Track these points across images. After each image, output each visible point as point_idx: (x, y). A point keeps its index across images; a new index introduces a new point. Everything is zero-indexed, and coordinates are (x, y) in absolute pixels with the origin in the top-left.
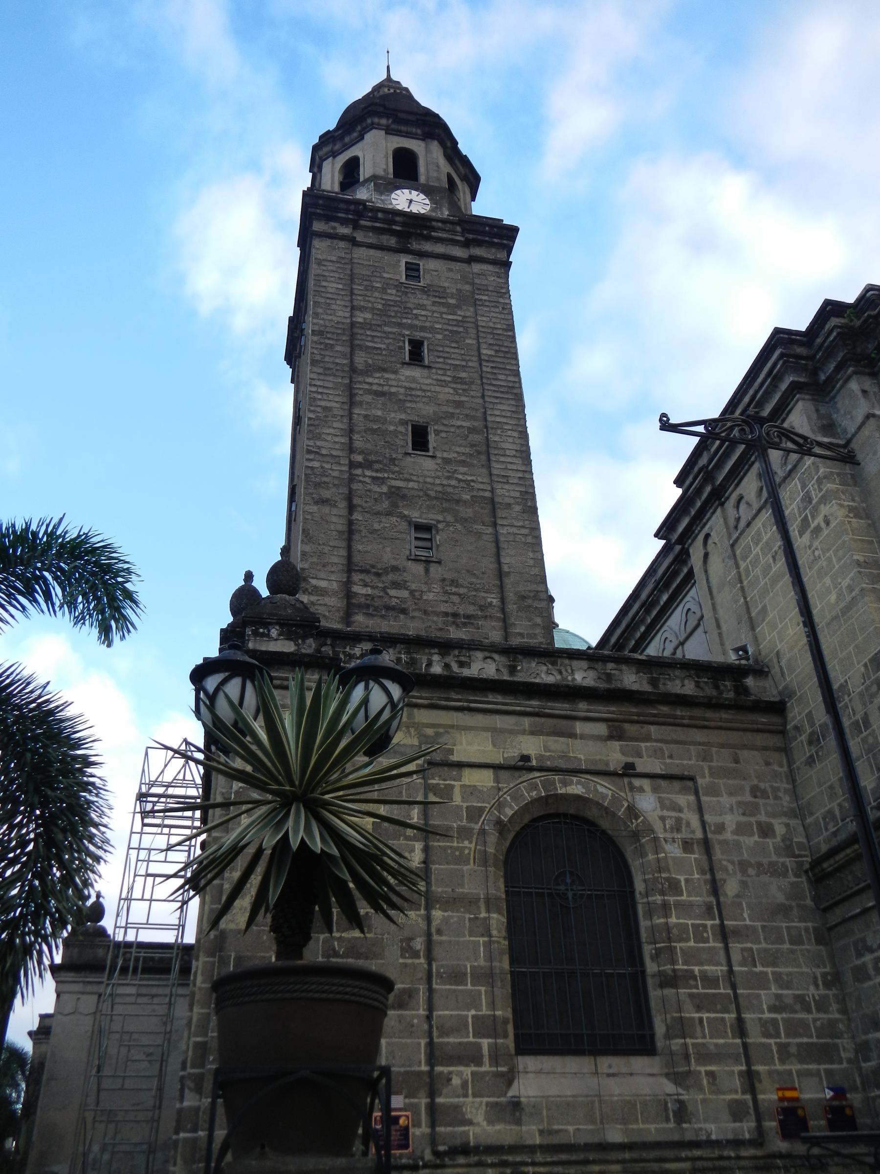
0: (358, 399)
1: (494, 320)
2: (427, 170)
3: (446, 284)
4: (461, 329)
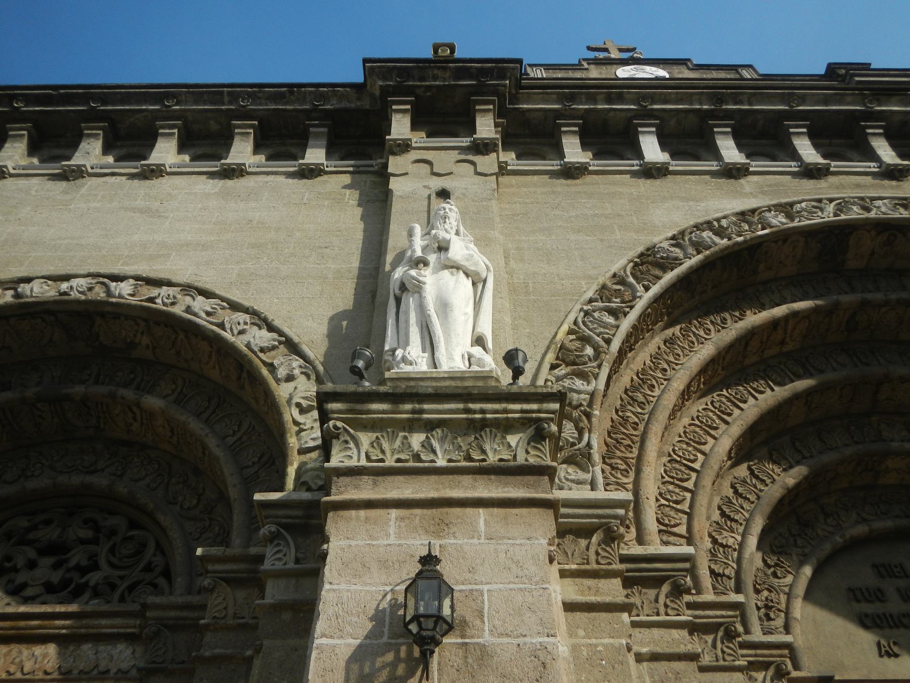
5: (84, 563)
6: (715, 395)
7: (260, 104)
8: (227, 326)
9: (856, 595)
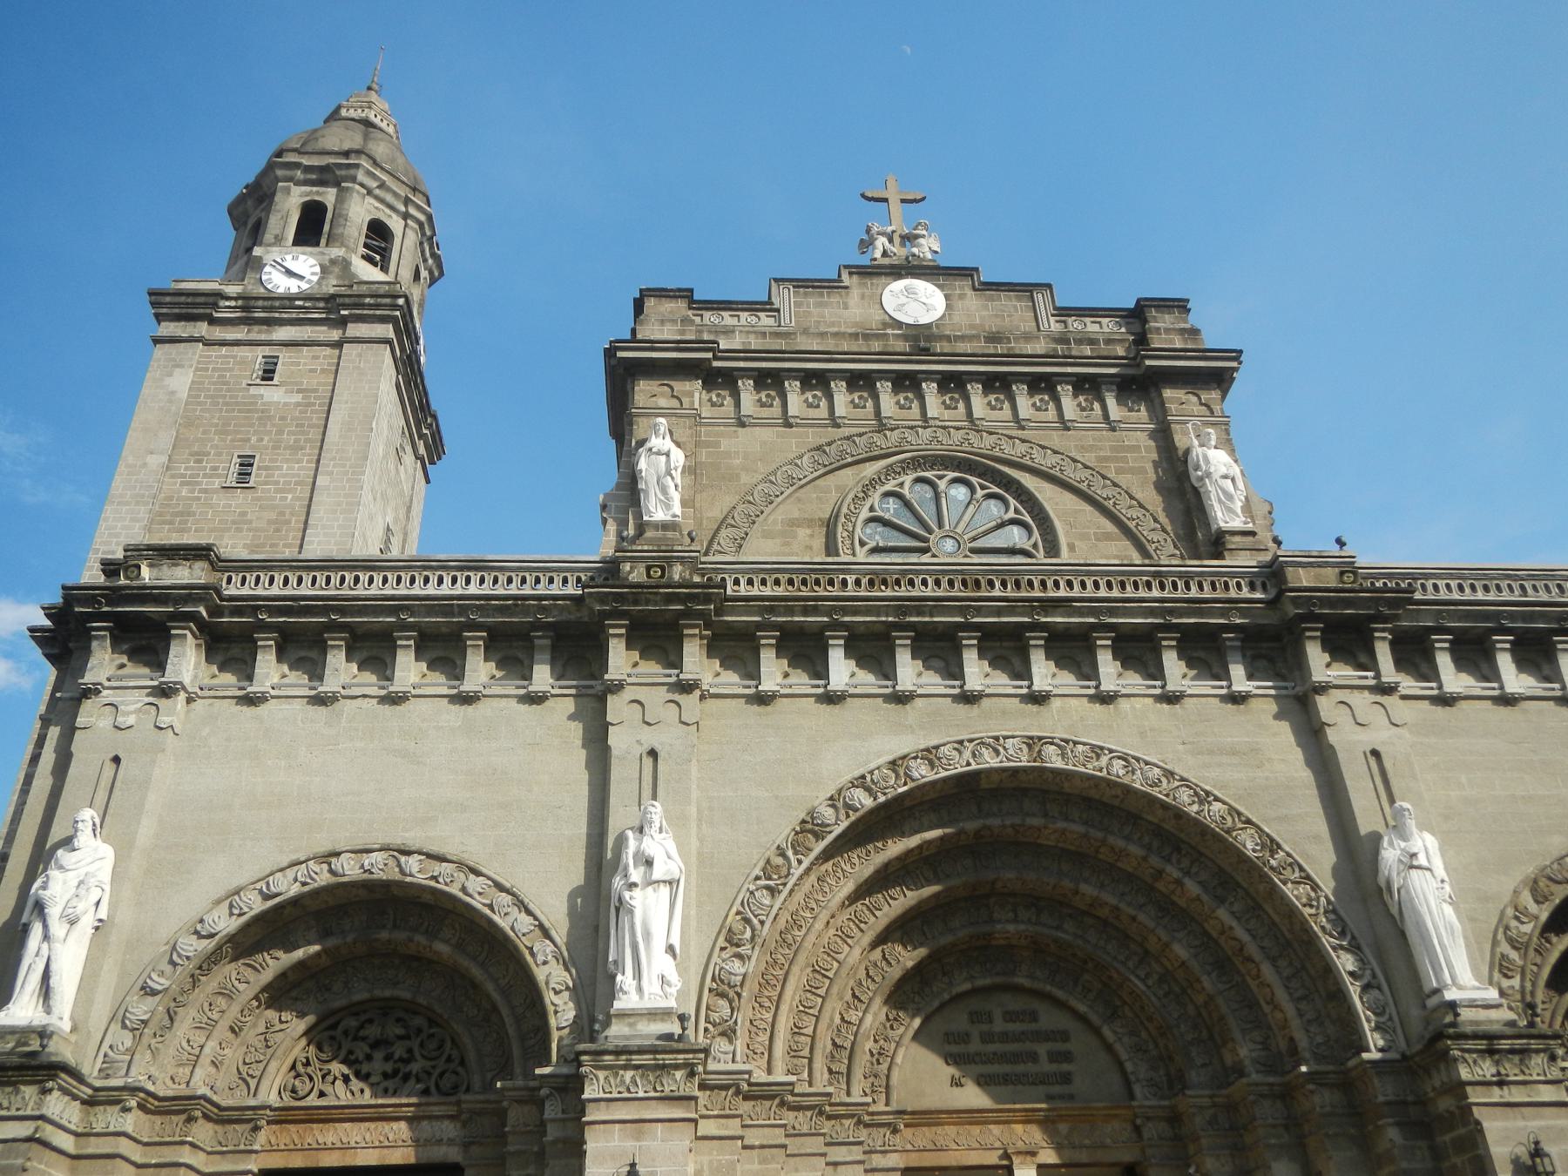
6: (859, 904)
7: (488, 617)
8: (496, 909)
9: (950, 1038)
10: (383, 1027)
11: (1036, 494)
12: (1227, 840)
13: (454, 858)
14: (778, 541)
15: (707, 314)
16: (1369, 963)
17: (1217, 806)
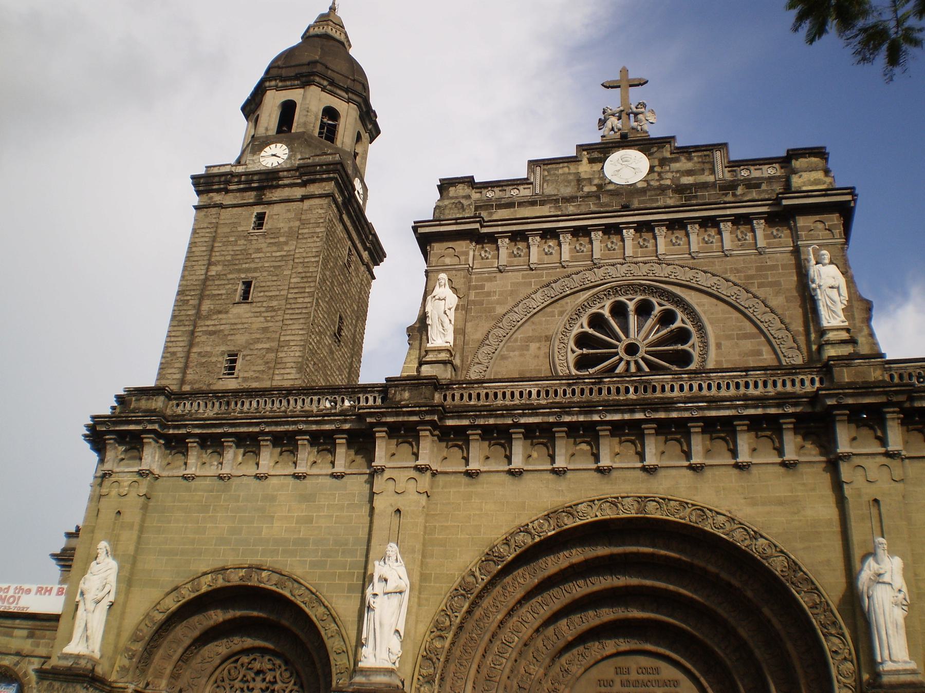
0: (197, 340)
1: (308, 250)
2: (299, 118)
3: (282, 225)
4: (283, 263)
5: (272, 680)
10: (262, 663)
11: (696, 308)
12: (764, 565)
13: (286, 573)
14: (517, 353)
15: (484, 191)
16: (848, 645)
17: (761, 541)
